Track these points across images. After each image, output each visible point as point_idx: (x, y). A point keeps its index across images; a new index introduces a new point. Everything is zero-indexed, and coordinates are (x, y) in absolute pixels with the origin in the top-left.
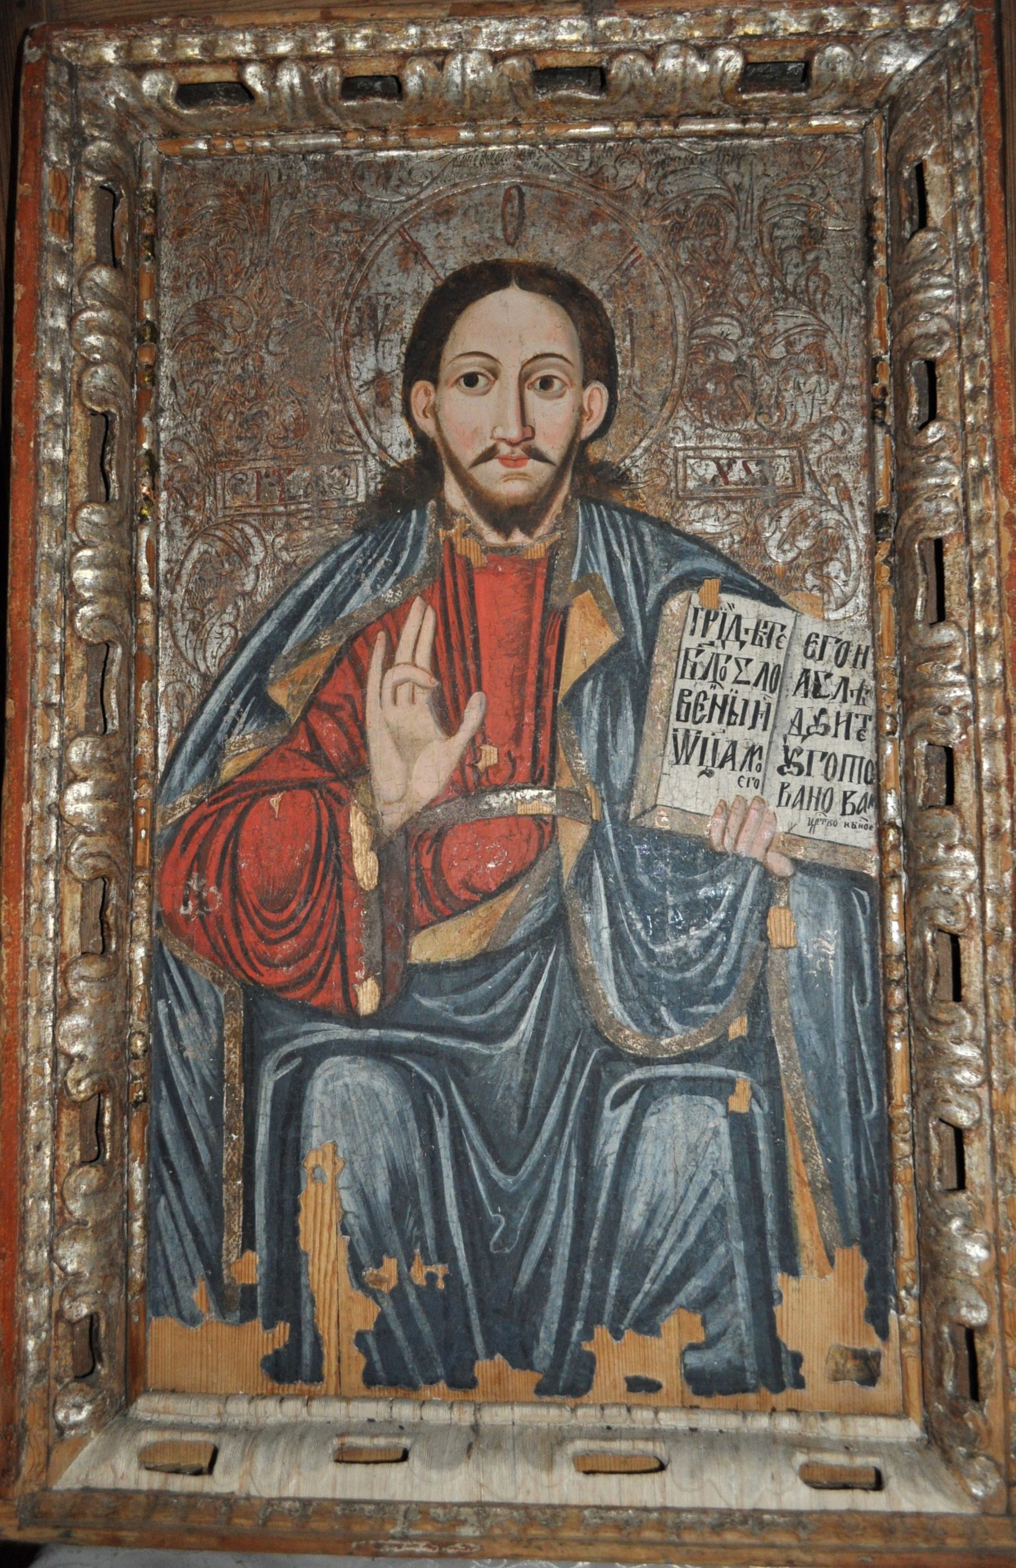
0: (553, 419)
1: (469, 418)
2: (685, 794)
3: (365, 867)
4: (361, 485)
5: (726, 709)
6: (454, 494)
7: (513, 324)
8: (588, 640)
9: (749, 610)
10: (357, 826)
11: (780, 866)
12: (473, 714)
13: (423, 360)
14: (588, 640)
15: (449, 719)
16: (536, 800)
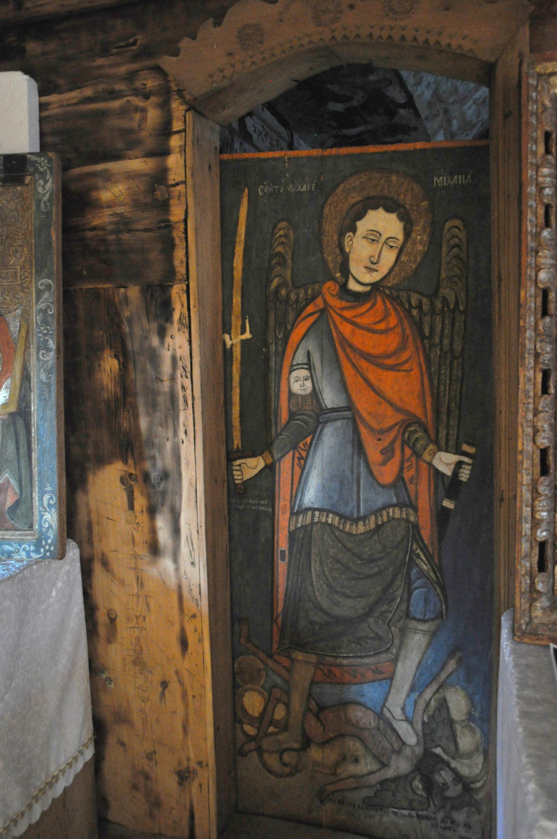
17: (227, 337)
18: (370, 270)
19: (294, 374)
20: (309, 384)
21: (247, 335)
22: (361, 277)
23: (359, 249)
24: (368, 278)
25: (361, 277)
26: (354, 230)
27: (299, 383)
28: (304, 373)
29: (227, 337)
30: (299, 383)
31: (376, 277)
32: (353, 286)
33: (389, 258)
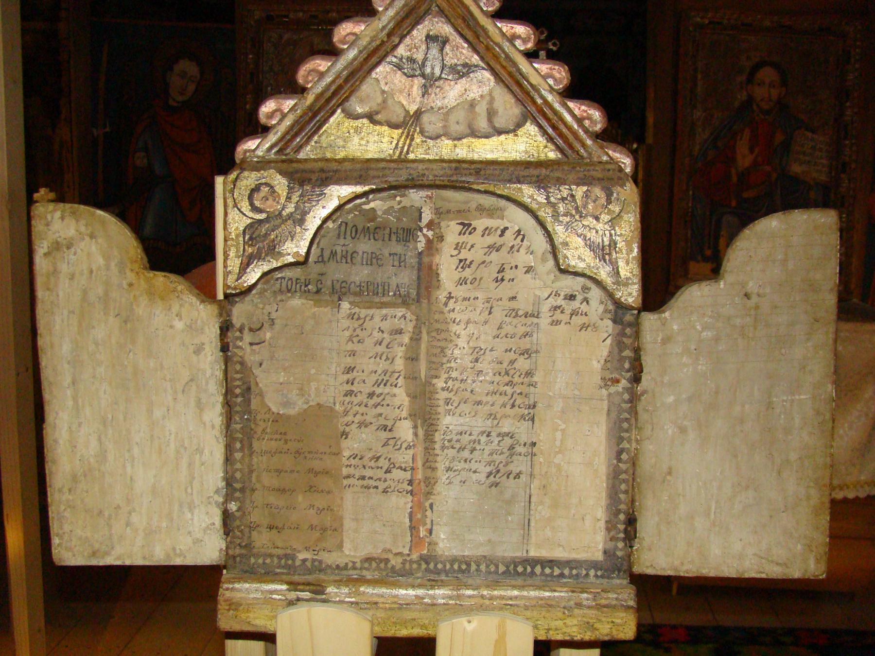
0: (774, 93)
1: (759, 92)
2: (796, 169)
3: (735, 179)
4: (737, 104)
5: (804, 154)
6: (755, 107)
7: (767, 74)
8: (779, 138)
9: (810, 135)
10: (733, 171)
11: (812, 183)
12: (756, 151)
13: (750, 79)
14: (779, 138)
15: (751, 151)
16: (767, 168)
17: (95, 130)
18: (182, 94)
19: (138, 154)
20: (145, 161)
21: (108, 130)
22: (176, 98)
23: (175, 81)
24: (180, 98)
25: (176, 98)
26: (172, 69)
27: (140, 160)
28: (143, 154)
29: (95, 130)
30: (140, 160)
31: (185, 98)
32: (171, 102)
33: (192, 88)
